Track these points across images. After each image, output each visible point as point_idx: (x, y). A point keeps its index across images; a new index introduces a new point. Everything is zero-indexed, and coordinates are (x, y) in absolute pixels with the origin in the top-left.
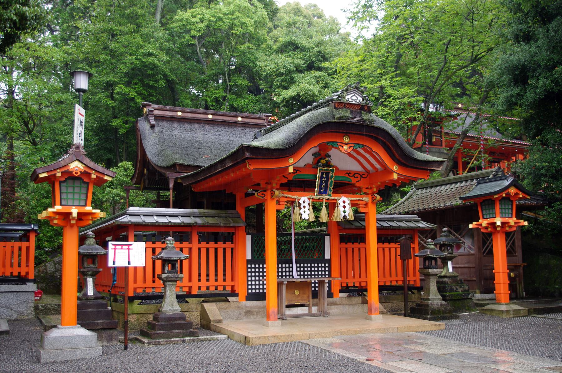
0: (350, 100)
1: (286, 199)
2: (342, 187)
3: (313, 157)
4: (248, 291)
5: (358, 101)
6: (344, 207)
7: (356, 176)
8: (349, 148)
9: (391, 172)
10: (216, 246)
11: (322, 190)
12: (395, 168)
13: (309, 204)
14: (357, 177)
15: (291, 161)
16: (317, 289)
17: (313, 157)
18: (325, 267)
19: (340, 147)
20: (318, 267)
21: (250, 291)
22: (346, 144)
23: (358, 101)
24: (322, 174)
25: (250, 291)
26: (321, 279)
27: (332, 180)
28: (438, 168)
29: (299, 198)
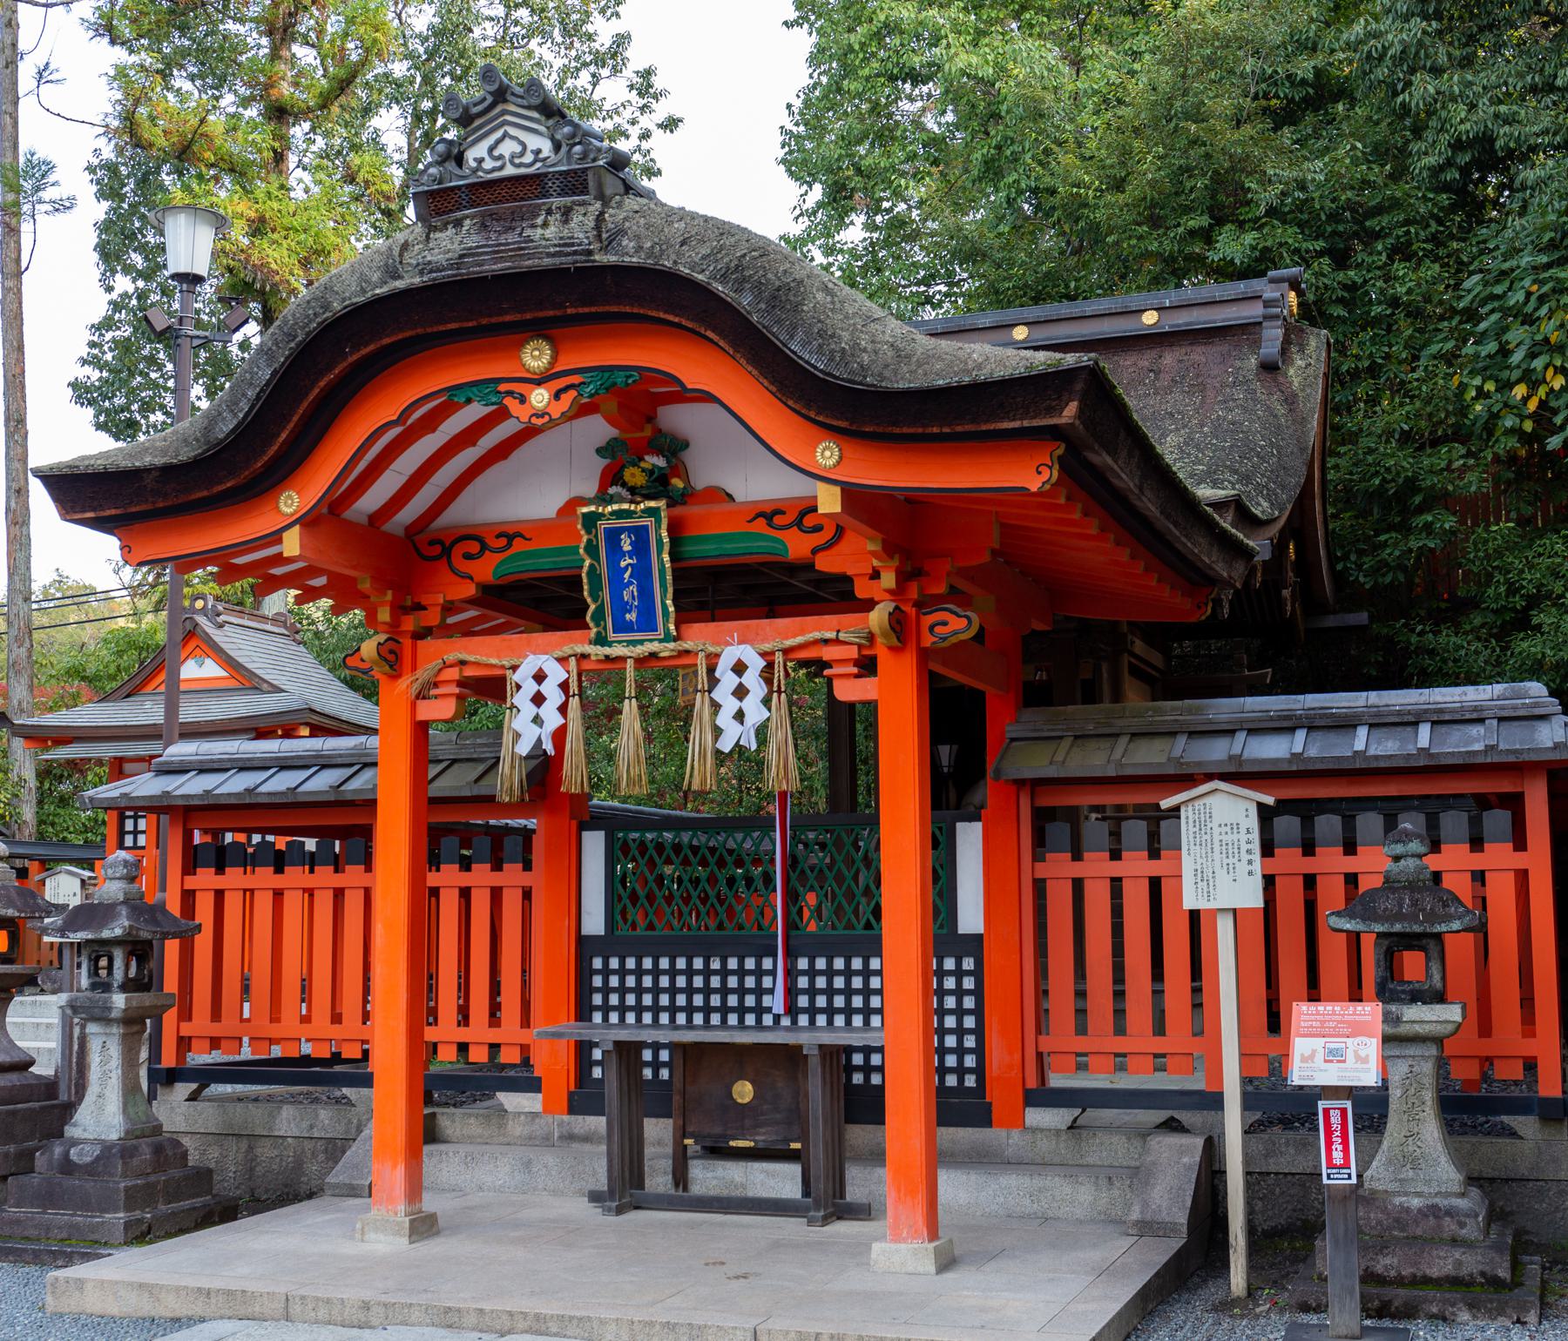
0: (489, 164)
1: (453, 674)
3: (601, 463)
5: (528, 158)
8: (557, 396)
10: (497, 879)
13: (564, 686)
15: (290, 503)
17: (605, 462)
18: (959, 974)
22: (539, 381)
26: (624, 1035)
28: (1050, 411)
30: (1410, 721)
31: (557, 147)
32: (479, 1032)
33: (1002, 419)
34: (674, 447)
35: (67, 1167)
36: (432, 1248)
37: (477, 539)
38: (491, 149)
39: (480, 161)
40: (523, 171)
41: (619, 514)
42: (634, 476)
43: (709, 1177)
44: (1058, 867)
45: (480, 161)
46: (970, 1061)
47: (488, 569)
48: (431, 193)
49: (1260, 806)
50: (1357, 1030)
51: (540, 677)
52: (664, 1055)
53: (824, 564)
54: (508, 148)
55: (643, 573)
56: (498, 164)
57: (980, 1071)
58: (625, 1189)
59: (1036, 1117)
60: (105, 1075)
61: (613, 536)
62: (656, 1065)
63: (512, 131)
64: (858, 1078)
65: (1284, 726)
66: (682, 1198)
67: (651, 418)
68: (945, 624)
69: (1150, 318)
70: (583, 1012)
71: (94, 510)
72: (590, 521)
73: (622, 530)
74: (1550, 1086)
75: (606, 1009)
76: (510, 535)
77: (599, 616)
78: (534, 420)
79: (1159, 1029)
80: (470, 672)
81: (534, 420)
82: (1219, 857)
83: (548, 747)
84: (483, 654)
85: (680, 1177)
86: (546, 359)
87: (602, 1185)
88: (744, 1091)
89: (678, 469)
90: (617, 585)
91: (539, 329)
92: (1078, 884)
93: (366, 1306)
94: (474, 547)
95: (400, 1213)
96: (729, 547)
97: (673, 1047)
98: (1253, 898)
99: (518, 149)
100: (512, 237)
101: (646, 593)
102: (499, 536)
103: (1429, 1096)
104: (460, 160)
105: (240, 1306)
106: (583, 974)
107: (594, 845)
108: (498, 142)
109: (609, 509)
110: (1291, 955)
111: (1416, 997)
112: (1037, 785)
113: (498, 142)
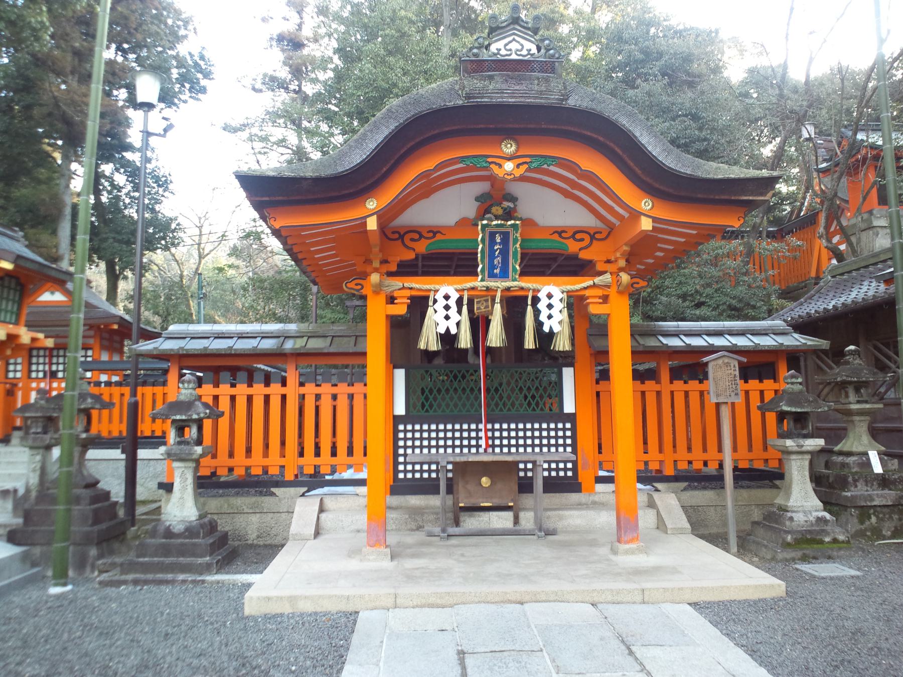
0: (503, 52)
1: (408, 293)
2: (541, 264)
4: (521, 462)
5: (524, 52)
6: (550, 306)
7: (578, 236)
8: (518, 166)
9: (636, 215)
11: (497, 271)
12: (646, 204)
14: (582, 240)
15: (372, 204)
16: (530, 474)
17: (478, 204)
18: (564, 429)
19: (492, 166)
20: (533, 430)
21: (401, 476)
22: (509, 159)
23: (524, 52)
24: (492, 235)
25: (401, 476)
27: (516, 247)
28: (762, 194)
29: (437, 287)
33: (741, 195)
37: (418, 233)
38: (506, 45)
39: (499, 50)
40: (521, 58)
41: (497, 226)
45: (499, 50)
47: (422, 247)
48: (472, 61)
49: (740, 363)
51: (550, 296)
53: (583, 255)
54: (514, 46)
55: (505, 253)
56: (509, 53)
57: (575, 469)
60: (184, 488)
61: (492, 235)
63: (517, 38)
68: (638, 283)
71: (269, 196)
72: (484, 226)
73: (497, 233)
76: (434, 232)
78: (506, 176)
79: (705, 450)
80: (414, 293)
81: (506, 176)
83: (453, 331)
86: (514, 148)
89: (515, 210)
90: (492, 257)
94: (416, 236)
96: (542, 245)
99: (520, 47)
102: (428, 232)
104: (487, 47)
108: (510, 42)
109: (509, 223)
113: (510, 42)
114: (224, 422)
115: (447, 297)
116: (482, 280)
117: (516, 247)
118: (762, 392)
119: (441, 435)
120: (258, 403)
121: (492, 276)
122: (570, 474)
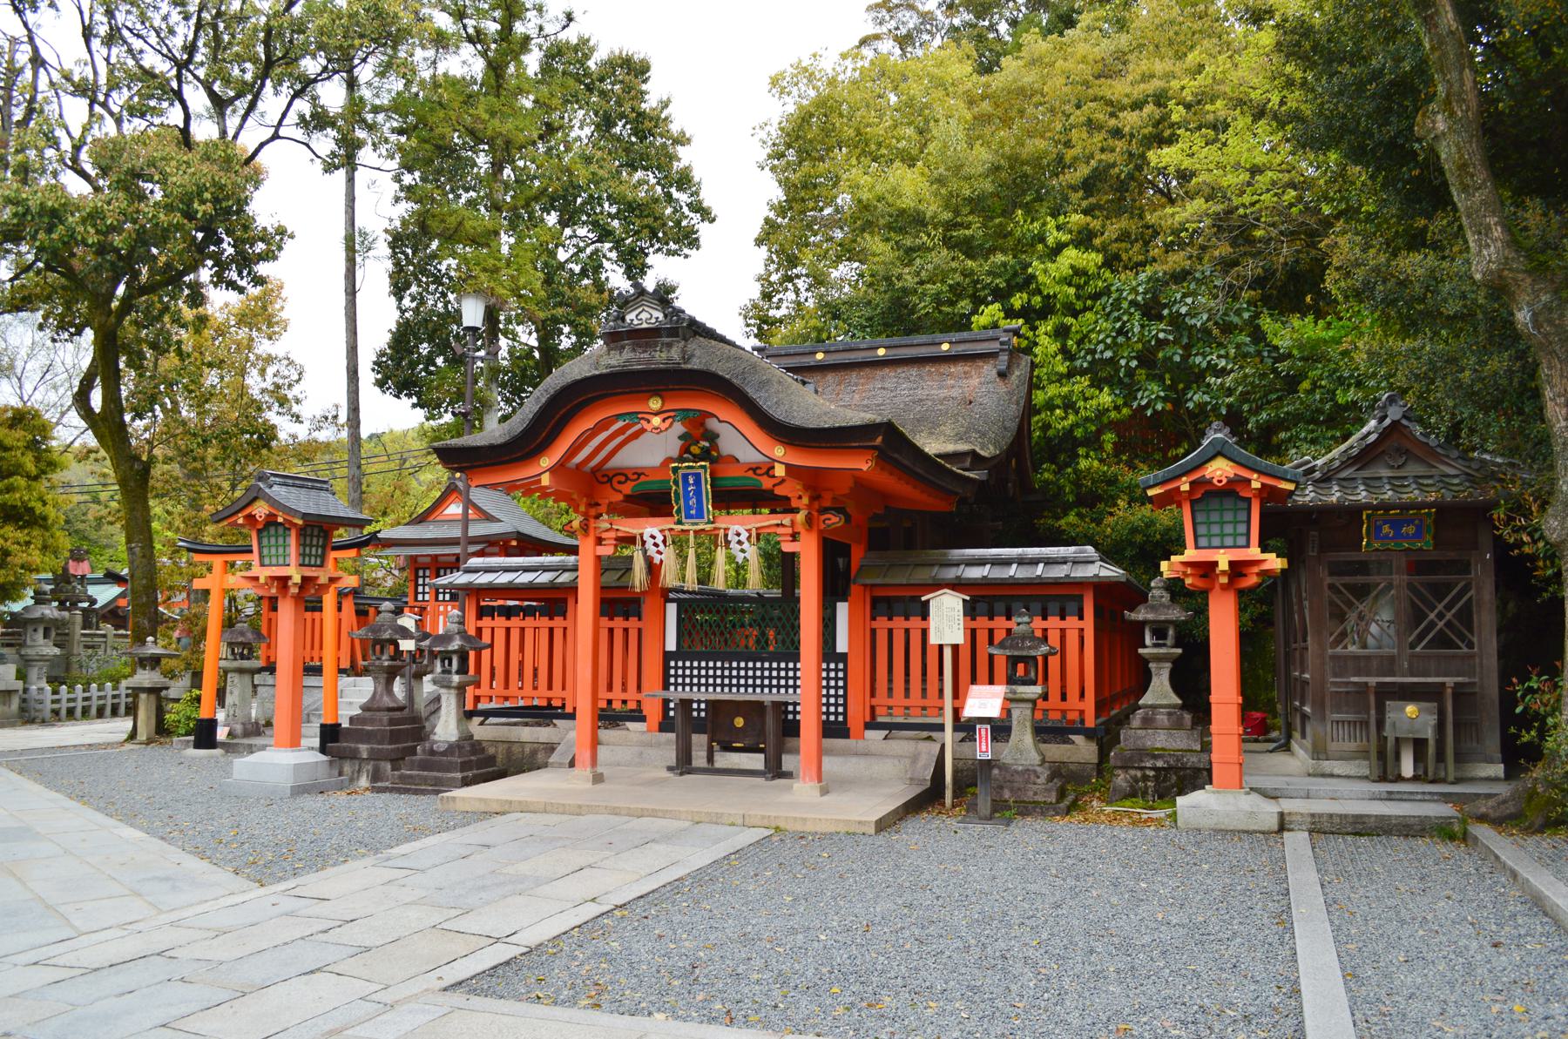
3: (680, 443)
15: (546, 462)
17: (680, 443)
18: (836, 670)
20: (779, 669)
22: (656, 414)
24: (685, 477)
26: (685, 696)
30: (1034, 562)
31: (665, 316)
32: (631, 694)
34: (713, 437)
35: (432, 752)
36: (599, 786)
37: (623, 474)
42: (695, 450)
43: (725, 760)
44: (882, 624)
46: (841, 709)
47: (628, 488)
50: (994, 696)
52: (703, 706)
55: (698, 493)
58: (684, 765)
59: (869, 734)
60: (448, 713)
61: (685, 477)
62: (699, 710)
64: (790, 717)
65: (981, 562)
66: (712, 770)
67: (702, 424)
69: (945, 347)
70: (666, 686)
72: (675, 470)
74: (1090, 722)
75: (676, 684)
76: (639, 473)
77: (679, 511)
82: (947, 619)
84: (627, 526)
85: (710, 759)
87: (673, 762)
88: (739, 722)
89: (715, 446)
90: (687, 499)
91: (656, 393)
92: (890, 631)
93: (580, 807)
94: (622, 479)
95: (588, 772)
97: (706, 702)
98: (958, 637)
100: (646, 355)
101: (699, 502)
103: (1028, 724)
104: (623, 319)
105: (525, 808)
106: (666, 668)
107: (672, 609)
110: (971, 666)
111: (1024, 683)
112: (873, 586)
114: (486, 654)
115: (653, 537)
116: (679, 522)
117: (707, 488)
118: (991, 632)
119: (758, 673)
120: (558, 635)
121: (689, 516)
122: (841, 718)
